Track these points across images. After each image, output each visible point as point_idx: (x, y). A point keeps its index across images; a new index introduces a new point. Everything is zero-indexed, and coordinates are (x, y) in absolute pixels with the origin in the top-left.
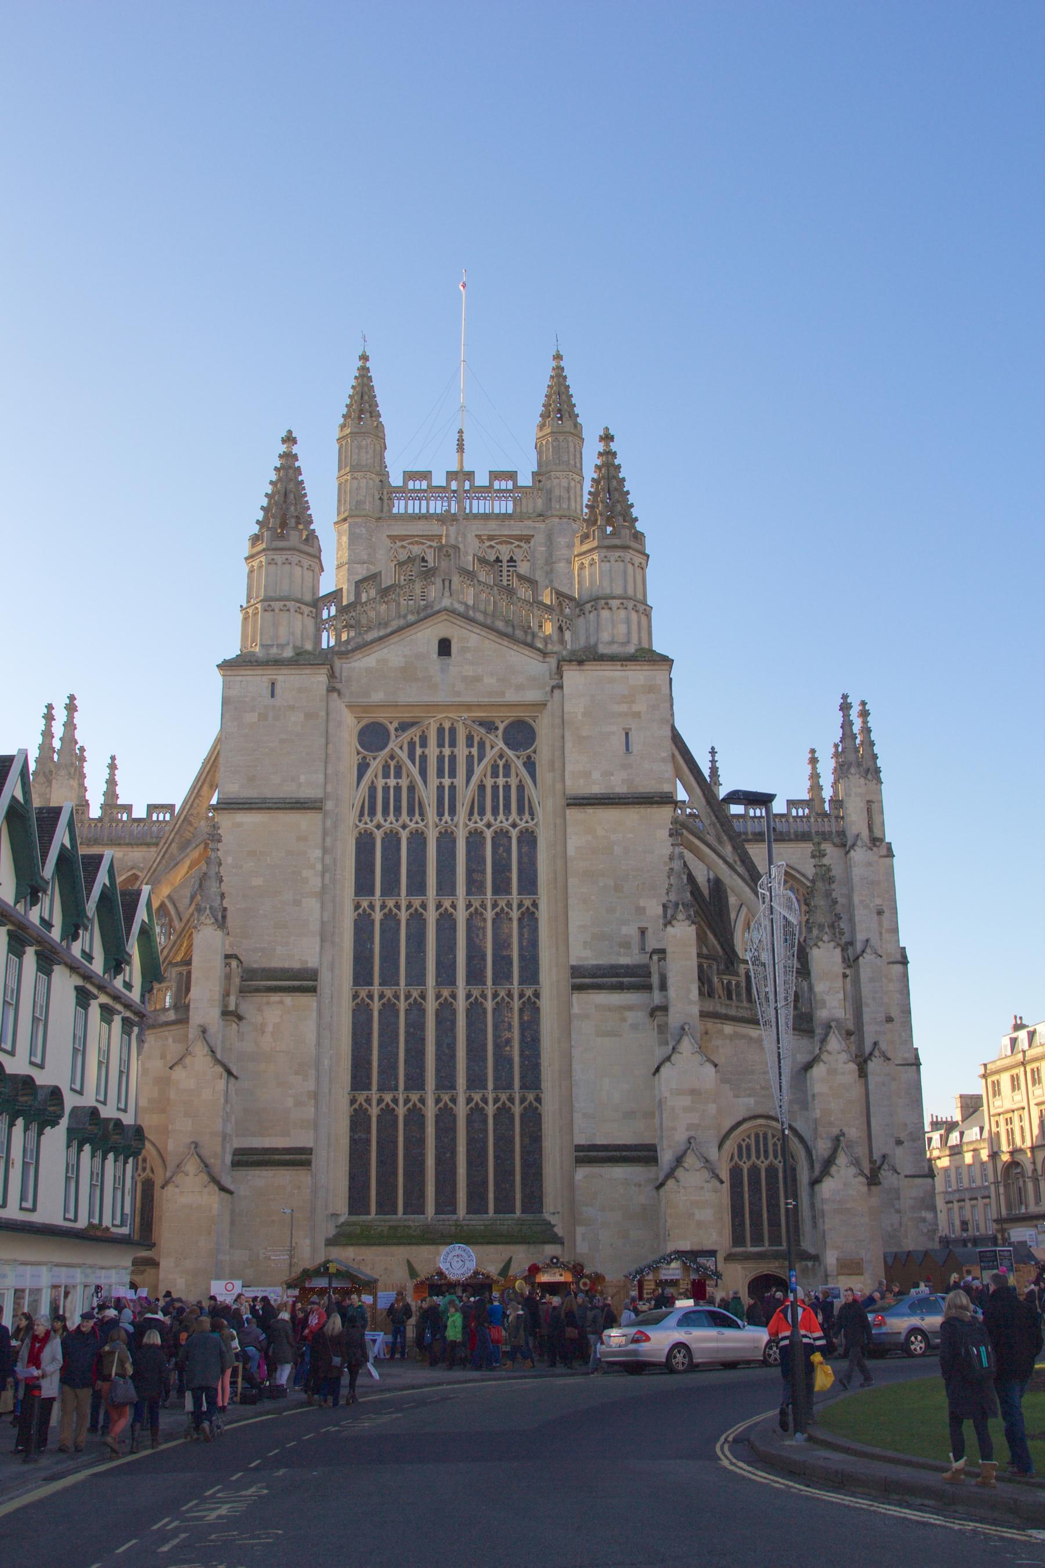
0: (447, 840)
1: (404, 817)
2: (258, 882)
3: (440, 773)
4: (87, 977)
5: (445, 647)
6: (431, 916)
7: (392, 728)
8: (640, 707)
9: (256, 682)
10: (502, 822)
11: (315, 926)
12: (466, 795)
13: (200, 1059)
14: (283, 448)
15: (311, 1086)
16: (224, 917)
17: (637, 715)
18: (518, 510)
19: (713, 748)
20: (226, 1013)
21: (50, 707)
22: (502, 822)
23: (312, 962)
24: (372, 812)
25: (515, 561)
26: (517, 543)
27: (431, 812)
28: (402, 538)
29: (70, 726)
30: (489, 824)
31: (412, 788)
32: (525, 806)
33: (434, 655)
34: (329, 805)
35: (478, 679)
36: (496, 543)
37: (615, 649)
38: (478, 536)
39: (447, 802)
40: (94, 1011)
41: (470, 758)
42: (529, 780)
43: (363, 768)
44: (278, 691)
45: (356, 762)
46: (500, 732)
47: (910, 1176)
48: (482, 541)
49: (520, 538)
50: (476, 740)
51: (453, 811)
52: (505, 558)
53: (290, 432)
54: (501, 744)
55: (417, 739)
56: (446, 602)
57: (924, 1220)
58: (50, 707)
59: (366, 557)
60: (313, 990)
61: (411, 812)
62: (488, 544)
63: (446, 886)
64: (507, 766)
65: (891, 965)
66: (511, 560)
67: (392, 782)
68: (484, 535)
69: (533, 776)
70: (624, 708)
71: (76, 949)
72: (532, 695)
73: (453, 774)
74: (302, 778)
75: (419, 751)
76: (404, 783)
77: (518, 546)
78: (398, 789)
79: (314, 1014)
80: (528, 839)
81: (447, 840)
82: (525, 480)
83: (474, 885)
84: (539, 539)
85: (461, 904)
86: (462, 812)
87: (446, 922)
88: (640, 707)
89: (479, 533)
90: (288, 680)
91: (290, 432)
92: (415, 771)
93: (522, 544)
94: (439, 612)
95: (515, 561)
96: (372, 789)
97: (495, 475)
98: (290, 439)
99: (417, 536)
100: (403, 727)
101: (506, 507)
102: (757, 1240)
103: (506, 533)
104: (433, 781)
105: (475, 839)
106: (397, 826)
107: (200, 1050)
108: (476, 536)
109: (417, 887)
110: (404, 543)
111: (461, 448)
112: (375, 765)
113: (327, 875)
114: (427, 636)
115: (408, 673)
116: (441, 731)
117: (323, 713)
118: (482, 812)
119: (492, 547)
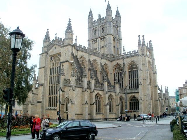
5: (55, 47)
9: (42, 56)
14: (47, 30)
57: (149, 106)
60: (42, 86)
82: (105, 18)
90: (43, 55)
98: (48, 29)
115: (53, 52)
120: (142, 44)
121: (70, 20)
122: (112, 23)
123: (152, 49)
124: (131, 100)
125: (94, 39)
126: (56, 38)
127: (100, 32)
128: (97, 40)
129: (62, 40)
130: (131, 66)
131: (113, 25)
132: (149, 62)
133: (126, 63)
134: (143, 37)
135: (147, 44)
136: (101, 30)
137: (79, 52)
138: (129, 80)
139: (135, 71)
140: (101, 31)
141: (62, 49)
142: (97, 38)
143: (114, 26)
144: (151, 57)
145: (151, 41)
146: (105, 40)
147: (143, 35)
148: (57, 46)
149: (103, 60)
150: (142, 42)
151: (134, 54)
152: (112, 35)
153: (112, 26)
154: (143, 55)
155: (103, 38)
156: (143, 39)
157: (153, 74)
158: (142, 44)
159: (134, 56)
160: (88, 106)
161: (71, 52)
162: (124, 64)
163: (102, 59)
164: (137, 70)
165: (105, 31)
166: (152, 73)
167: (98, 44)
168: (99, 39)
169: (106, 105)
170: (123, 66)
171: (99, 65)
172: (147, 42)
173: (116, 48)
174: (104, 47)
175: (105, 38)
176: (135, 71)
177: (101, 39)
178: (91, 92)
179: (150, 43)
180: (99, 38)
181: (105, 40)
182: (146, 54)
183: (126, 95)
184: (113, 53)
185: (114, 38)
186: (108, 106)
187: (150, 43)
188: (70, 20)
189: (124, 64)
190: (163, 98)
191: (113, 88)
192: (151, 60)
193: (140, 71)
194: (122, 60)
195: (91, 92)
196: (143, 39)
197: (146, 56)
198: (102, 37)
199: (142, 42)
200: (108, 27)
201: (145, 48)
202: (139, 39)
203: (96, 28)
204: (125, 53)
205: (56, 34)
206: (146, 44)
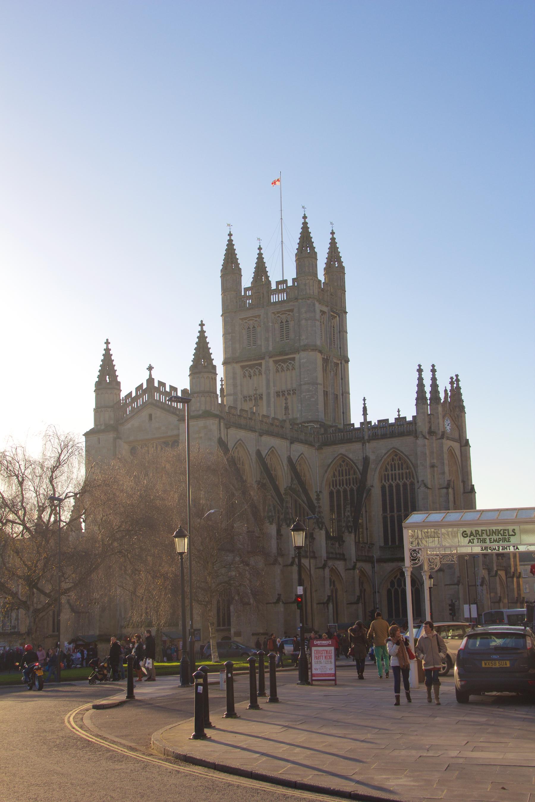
5: (150, 416)
18: (288, 298)
19: (364, 398)
25: (288, 322)
26: (288, 313)
28: (245, 319)
36: (281, 315)
38: (273, 313)
47: (447, 585)
48: (275, 315)
52: (284, 321)
53: (107, 340)
59: (230, 331)
62: (277, 315)
65: (441, 490)
66: (287, 321)
68: (275, 312)
77: (289, 314)
82: (290, 284)
89: (273, 311)
91: (107, 340)
93: (290, 313)
94: (147, 405)
95: (288, 322)
97: (278, 283)
98: (107, 343)
101: (283, 297)
102: (224, 625)
103: (283, 310)
108: (272, 313)
110: (246, 321)
114: (145, 414)
119: (279, 316)
120: (428, 396)
121: (202, 325)
122: (317, 304)
123: (462, 409)
124: (392, 583)
125: (250, 360)
126: (150, 380)
128: (260, 365)
129: (179, 394)
130: (389, 468)
131: (321, 311)
132: (451, 451)
133: (372, 457)
134: (433, 371)
135: (446, 391)
136: (277, 326)
137: (232, 431)
138: (385, 518)
139: (405, 485)
142: (263, 358)
143: (323, 313)
144: (457, 436)
146: (293, 368)
147: (433, 366)
148: (158, 413)
149: (293, 446)
150: (428, 389)
152: (320, 352)
153: (318, 315)
154: (431, 432)
155: (284, 361)
156: (434, 379)
157: (464, 493)
158: (428, 396)
159: (401, 434)
160: (282, 609)
162: (366, 461)
163: (291, 443)
164: (412, 484)
165: (292, 336)
166: (462, 490)
167: (268, 381)
168: (271, 360)
169: (324, 603)
170: (361, 468)
171: (286, 468)
172: (444, 385)
173: (331, 397)
174: (289, 394)
175: (293, 359)
176: (405, 485)
177: (276, 362)
178: (287, 566)
179: (455, 381)
180: (270, 357)
181: (293, 368)
182: (441, 429)
183: (373, 567)
184: (321, 416)
185: (326, 361)
186: (331, 606)
187: (455, 381)
188: (202, 325)
189: (366, 461)
190: (496, 572)
191: (340, 545)
192: (456, 446)
193: (423, 489)
194: (357, 446)
195: (287, 566)
196: (434, 379)
197: (442, 437)
198: (281, 354)
199: (428, 389)
200: (303, 322)
201: (440, 409)
202: (420, 379)
203: (256, 317)
204: (370, 422)
205: (150, 368)
206: (442, 396)
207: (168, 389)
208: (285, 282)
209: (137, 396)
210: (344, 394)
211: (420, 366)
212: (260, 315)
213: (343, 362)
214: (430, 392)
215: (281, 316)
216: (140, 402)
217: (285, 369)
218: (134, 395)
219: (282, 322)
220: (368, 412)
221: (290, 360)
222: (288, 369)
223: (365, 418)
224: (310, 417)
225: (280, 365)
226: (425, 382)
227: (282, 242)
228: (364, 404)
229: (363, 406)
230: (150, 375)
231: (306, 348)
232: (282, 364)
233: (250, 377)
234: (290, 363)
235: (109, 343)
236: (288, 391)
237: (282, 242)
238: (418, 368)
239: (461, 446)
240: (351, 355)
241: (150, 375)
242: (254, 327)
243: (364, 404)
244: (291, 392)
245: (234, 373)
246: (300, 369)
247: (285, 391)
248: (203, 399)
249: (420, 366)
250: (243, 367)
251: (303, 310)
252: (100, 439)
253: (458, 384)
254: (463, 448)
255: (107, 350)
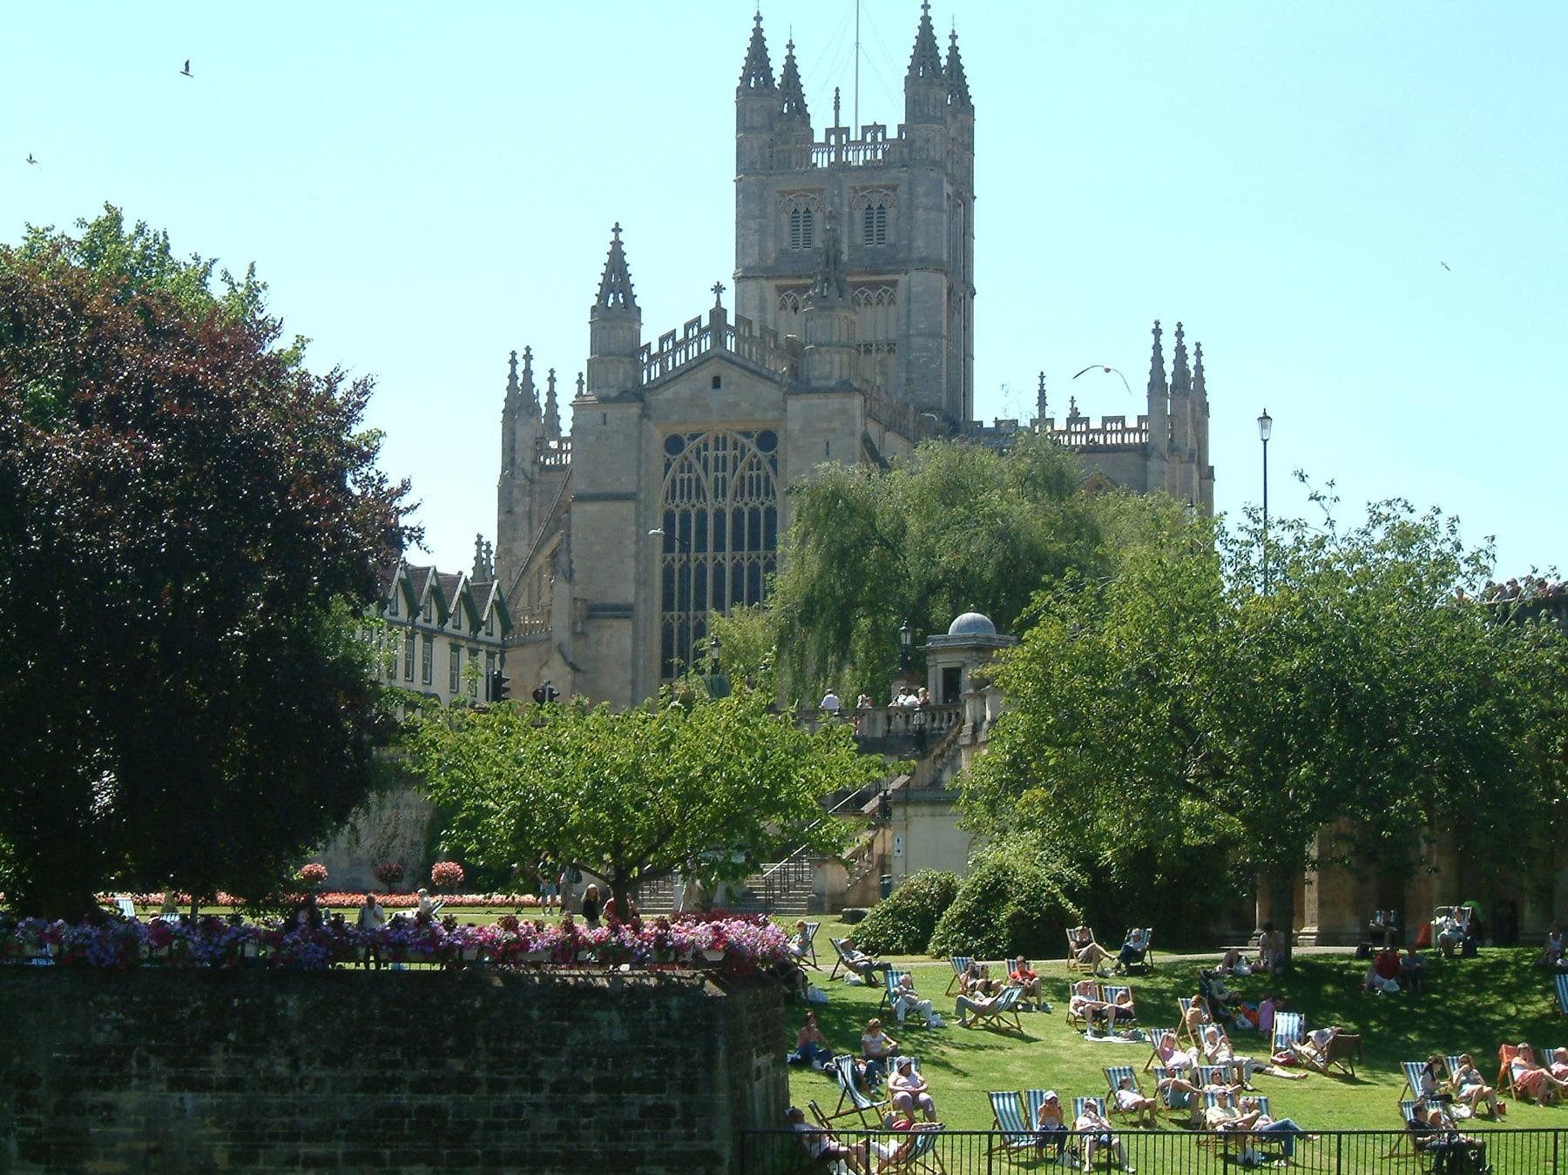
0: (720, 515)
1: (693, 500)
2: (597, 548)
3: (716, 470)
4: (457, 637)
5: (716, 383)
6: (710, 566)
7: (685, 438)
8: (836, 424)
10: (755, 502)
11: (631, 575)
12: (732, 483)
13: (557, 661)
15: (629, 676)
16: (571, 576)
17: (834, 430)
20: (575, 633)
21: (513, 354)
22: (755, 502)
23: (631, 599)
24: (673, 498)
27: (710, 495)
29: (528, 372)
30: (748, 503)
31: (698, 480)
32: (770, 491)
33: (710, 389)
34: (642, 495)
35: (737, 404)
37: (822, 383)
39: (720, 490)
40: (464, 653)
41: (735, 457)
42: (771, 474)
43: (668, 466)
44: (608, 420)
45: (663, 464)
46: (754, 439)
49: (887, 187)
50: (739, 445)
51: (724, 495)
52: (875, 206)
53: (617, 224)
54: (754, 449)
55: (702, 446)
56: (717, 350)
58: (513, 354)
61: (698, 497)
63: (719, 546)
64: (759, 462)
67: (686, 476)
69: (776, 470)
70: (825, 425)
71: (448, 627)
72: (772, 415)
73: (724, 470)
74: (623, 480)
75: (703, 454)
76: (693, 476)
78: (689, 480)
79: (630, 632)
80: (771, 513)
81: (720, 515)
82: (892, 134)
83: (737, 545)
84: (903, 191)
85: (728, 558)
86: (729, 494)
87: (720, 569)
88: (836, 424)
91: (617, 224)
92: (698, 467)
93: (889, 193)
94: (712, 358)
96: (674, 481)
99: (803, 190)
100: (694, 437)
104: (712, 474)
105: (738, 515)
106: (689, 506)
107: (557, 658)
109: (701, 547)
110: (791, 197)
111: (837, 107)
112: (675, 465)
113: (642, 543)
114: (705, 374)
116: (717, 439)
117: (636, 435)
118: (742, 495)
119: (864, 196)
120: (1169, 380)
125: (800, 277)
126: (718, 313)
127: (851, 231)
134: (1180, 334)
136: (859, 215)
140: (859, 226)
141: (795, 405)
145: (1198, 345)
146: (892, 301)
147: (1180, 325)
148: (730, 375)
150: (1169, 367)
151: (1114, 439)
154: (1173, 449)
155: (873, 286)
158: (1169, 380)
161: (859, 436)
165: (891, 237)
175: (894, 284)
181: (892, 301)
196: (1180, 350)
199: (1169, 367)
202: (1157, 348)
207: (757, 333)
208: (884, 128)
209: (686, 341)
210: (967, 359)
211: (1157, 323)
212: (824, 189)
213: (968, 296)
214: (1173, 374)
215: (869, 196)
216: (693, 352)
217: (874, 301)
218: (680, 336)
219: (869, 207)
220: (1047, 401)
221: (884, 284)
222: (880, 302)
223: (1042, 414)
224: (926, 400)
225: (862, 292)
226: (1163, 353)
227: (857, 43)
228: (1042, 385)
229: (1039, 388)
230: (718, 302)
231: (923, 264)
232: (869, 292)
233: (796, 309)
234: (886, 291)
235: (621, 230)
236: (865, 345)
237: (857, 43)
238: (1154, 327)
239: (1201, 478)
240: (978, 281)
241: (718, 302)
242: (808, 211)
243: (1042, 385)
244: (886, 348)
245: (763, 300)
246: (909, 304)
247: (871, 345)
248: (836, 357)
249: (1157, 323)
250: (781, 290)
251: (921, 190)
252: (608, 417)
253: (1199, 361)
254: (1203, 481)
255: (617, 244)
